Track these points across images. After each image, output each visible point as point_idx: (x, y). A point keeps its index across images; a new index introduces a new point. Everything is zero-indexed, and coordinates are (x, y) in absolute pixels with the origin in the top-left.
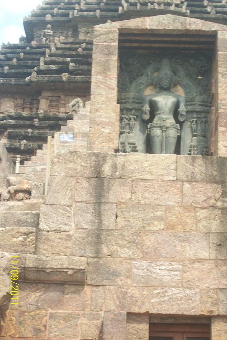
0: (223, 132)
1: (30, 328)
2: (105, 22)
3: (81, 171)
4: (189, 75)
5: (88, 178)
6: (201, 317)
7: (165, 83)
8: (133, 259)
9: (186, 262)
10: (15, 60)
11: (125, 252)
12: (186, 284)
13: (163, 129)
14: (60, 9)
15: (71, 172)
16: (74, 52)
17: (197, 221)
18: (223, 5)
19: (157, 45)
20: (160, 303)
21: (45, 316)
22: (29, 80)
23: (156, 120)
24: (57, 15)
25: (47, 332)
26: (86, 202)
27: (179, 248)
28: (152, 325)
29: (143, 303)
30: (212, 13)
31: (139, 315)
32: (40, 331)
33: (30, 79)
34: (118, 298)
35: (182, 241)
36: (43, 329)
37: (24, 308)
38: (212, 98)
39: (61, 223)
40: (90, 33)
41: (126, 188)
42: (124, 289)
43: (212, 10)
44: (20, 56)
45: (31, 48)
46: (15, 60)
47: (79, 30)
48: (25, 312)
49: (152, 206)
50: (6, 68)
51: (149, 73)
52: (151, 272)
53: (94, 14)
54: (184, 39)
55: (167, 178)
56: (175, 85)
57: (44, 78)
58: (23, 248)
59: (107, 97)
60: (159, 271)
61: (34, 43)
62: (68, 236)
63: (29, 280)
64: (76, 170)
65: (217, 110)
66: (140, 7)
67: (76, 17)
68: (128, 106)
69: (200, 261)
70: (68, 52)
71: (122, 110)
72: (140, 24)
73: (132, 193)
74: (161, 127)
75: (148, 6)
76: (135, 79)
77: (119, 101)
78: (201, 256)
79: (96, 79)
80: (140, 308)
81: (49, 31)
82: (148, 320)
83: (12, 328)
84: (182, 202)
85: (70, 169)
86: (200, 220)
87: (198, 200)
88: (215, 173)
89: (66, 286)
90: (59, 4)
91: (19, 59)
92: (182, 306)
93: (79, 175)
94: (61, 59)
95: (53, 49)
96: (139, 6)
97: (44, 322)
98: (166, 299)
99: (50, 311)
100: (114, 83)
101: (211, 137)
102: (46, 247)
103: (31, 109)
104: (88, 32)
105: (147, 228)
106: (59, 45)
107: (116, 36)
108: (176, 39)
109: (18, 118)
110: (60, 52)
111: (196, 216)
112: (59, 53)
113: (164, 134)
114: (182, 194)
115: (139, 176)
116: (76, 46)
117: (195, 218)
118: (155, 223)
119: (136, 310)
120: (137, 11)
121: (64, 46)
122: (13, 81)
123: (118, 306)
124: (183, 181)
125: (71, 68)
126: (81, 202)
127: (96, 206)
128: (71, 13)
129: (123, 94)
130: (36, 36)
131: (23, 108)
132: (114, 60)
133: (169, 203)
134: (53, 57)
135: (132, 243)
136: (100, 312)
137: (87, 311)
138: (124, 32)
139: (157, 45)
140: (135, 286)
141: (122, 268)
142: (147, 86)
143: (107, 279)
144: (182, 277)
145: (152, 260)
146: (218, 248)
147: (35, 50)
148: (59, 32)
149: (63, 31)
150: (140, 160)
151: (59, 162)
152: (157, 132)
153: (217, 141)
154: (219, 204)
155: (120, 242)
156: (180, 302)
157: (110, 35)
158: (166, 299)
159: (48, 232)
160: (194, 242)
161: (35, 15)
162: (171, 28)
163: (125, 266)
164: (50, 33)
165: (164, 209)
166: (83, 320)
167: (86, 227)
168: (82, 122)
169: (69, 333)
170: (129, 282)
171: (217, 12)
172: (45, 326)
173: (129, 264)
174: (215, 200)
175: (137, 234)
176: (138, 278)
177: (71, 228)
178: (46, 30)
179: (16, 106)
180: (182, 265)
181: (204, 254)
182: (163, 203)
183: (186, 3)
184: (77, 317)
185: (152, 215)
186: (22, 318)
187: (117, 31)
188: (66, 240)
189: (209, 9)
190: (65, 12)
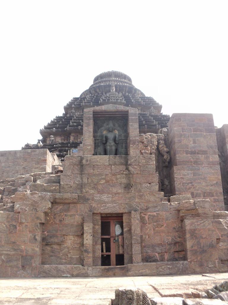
0: (132, 147)
1: (58, 220)
2: (94, 107)
3: (75, 163)
4: (119, 126)
5: (78, 165)
6: (119, 214)
7: (111, 129)
8: (94, 194)
9: (113, 194)
11: (92, 191)
12: (113, 202)
13: (111, 146)
15: (71, 163)
17: (117, 179)
19: (107, 116)
20: (104, 209)
21: (63, 215)
23: (108, 144)
24: (76, 105)
25: (64, 221)
26: (77, 174)
27: (111, 189)
28: (102, 217)
29: (98, 209)
31: (97, 214)
32: (61, 221)
33: (67, 129)
34: (89, 208)
35: (111, 186)
36: (63, 220)
37: (56, 213)
38: (128, 135)
39: (68, 182)
41: (91, 168)
42: (91, 205)
43: (134, 101)
45: (67, 117)
48: (56, 214)
49: (101, 175)
50: (58, 125)
51: (105, 126)
52: (101, 198)
54: (117, 113)
55: (106, 164)
56: (114, 130)
58: (55, 191)
59: (89, 135)
60: (103, 198)
61: (68, 115)
62: (71, 186)
63: (57, 202)
64: (73, 162)
65: (129, 139)
68: (97, 138)
69: (118, 193)
71: (95, 140)
72: (100, 108)
73: (93, 170)
74: (110, 146)
76: (100, 128)
77: (94, 137)
78: (119, 192)
79: (85, 128)
80: (97, 211)
82: (100, 216)
83: (52, 220)
84: (111, 173)
85: (71, 162)
86: (118, 179)
87: (117, 172)
88: (123, 162)
89: (70, 204)
91: (62, 122)
92: (112, 210)
93: (74, 164)
95: (75, 117)
97: (63, 218)
98: (106, 207)
99: (65, 213)
100: (92, 130)
101: (128, 148)
102: (63, 191)
103: (67, 140)
105: (99, 183)
106: (77, 116)
107: (92, 113)
108: (114, 113)
109: (62, 143)
110: (77, 119)
111: (116, 177)
113: (111, 148)
114: (111, 170)
115: (96, 164)
117: (116, 178)
118: (102, 180)
119: (96, 212)
123: (89, 211)
124: (111, 165)
126: (75, 174)
127: (81, 175)
129: (95, 134)
131: (64, 140)
132: (92, 121)
133: (106, 173)
135: (94, 188)
136: (83, 213)
137: (78, 213)
138: (95, 111)
139: (107, 116)
140: (95, 204)
141: (90, 197)
142: (104, 131)
143: (86, 201)
144: (112, 200)
145: (101, 194)
146: (125, 189)
147: (68, 118)
150: (96, 158)
151: (67, 160)
152: (108, 148)
153: (130, 150)
154: (125, 173)
155: (90, 188)
156: (111, 209)
157: (90, 113)
158: (106, 207)
159: (63, 185)
160: (116, 187)
161: (68, 105)
162: (112, 109)
163: (91, 196)
165: (105, 175)
166: (77, 216)
167: (77, 183)
169: (72, 221)
170: (93, 202)
172: (63, 219)
173: (93, 195)
174: (123, 171)
175: (96, 185)
176: (96, 201)
177: (72, 183)
178: (72, 111)
179: (61, 139)
180: (112, 195)
181: (120, 191)
182: (105, 173)
183: (124, 99)
184: (75, 215)
185: (101, 177)
186: (55, 217)
187: (92, 111)
188: (70, 188)
189: (133, 101)
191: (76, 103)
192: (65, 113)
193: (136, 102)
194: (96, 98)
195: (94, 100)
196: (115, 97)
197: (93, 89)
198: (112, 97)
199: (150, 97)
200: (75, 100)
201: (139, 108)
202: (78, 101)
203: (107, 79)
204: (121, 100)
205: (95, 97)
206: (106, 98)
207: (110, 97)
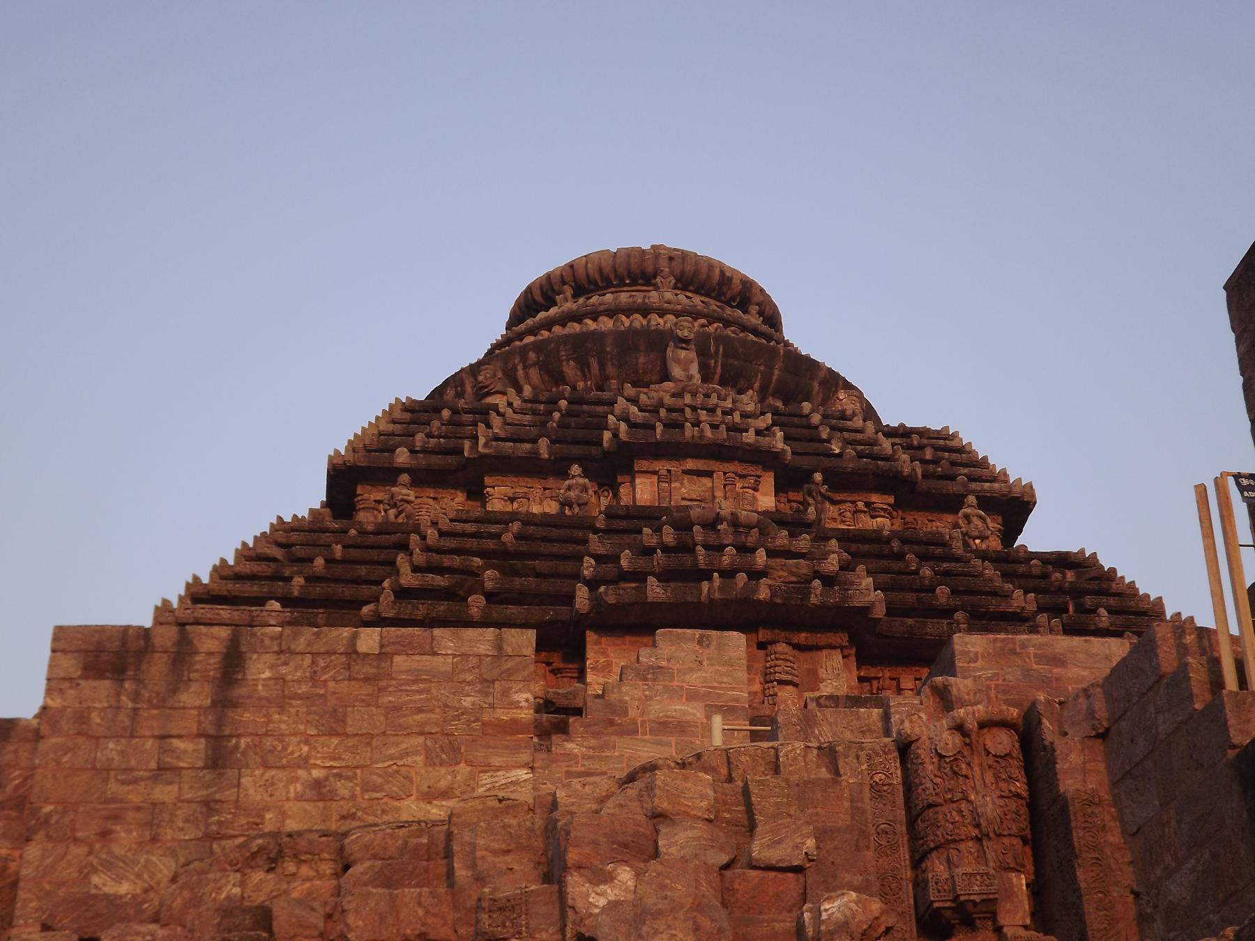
10: (320, 561)
14: (429, 435)
16: (490, 544)
18: (869, 438)
22: (372, 613)
24: (425, 451)
44: (334, 553)
45: (362, 532)
46: (320, 561)
47: (488, 492)
57: (418, 609)
67: (483, 456)
70: (472, 544)
75: (686, 429)
81: (405, 491)
90: (429, 425)
91: (330, 561)
94: (456, 561)
95: (431, 533)
96: (659, 428)
104: (511, 495)
106: (445, 525)
110: (451, 543)
116: (494, 529)
120: (658, 443)
122: (320, 616)
125: (489, 585)
128: (467, 444)
130: (361, 506)
134: (434, 555)
147: (372, 539)
149: (440, 496)
168: (649, 688)
178: (394, 489)
191: (419, 437)
192: (325, 500)
193: (860, 455)
194: (568, 414)
195: (561, 425)
196: (719, 412)
197: (532, 356)
198: (694, 409)
200: (407, 416)
201: (875, 498)
202: (436, 424)
203: (624, 297)
205: (563, 403)
206: (654, 410)
207: (681, 411)
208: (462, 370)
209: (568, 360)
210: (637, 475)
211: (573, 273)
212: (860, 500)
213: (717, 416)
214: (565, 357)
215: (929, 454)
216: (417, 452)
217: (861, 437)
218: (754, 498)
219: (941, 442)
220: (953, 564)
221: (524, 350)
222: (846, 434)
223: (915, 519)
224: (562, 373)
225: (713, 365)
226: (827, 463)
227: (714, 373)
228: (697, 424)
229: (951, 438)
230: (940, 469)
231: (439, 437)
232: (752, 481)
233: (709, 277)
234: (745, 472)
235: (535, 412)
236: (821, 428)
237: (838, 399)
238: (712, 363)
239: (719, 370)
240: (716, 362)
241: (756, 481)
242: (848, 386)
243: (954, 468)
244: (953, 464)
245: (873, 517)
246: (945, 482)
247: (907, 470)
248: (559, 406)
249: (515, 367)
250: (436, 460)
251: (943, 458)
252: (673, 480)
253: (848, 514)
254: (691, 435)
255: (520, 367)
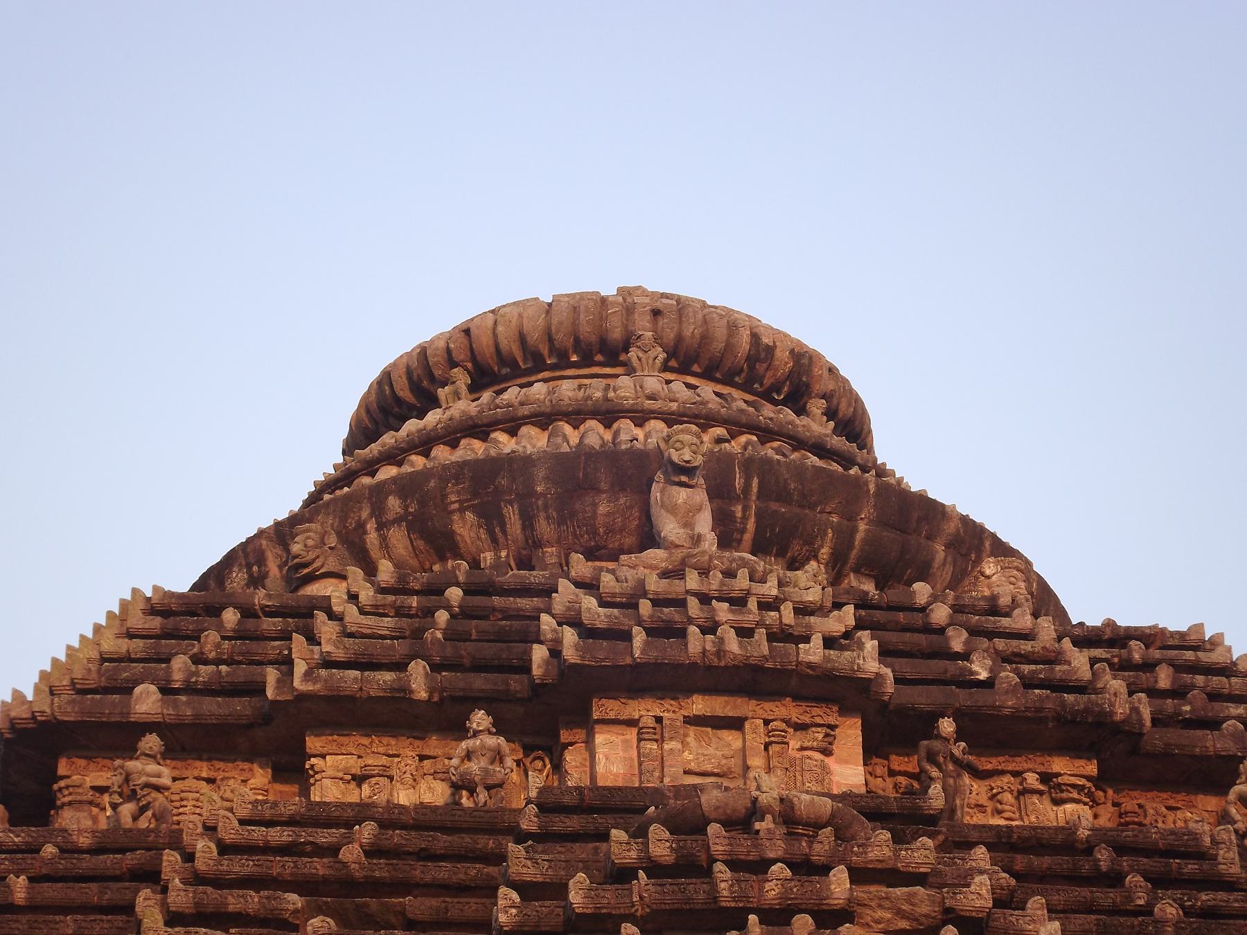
14: (199, 660)
16: (319, 867)
18: (1044, 648)
24: (190, 689)
30: (1001, 686)
40: (374, 780)
44: (12, 893)
45: (69, 850)
47: (312, 766)
53: (399, 679)
66: (646, 643)
67: (302, 697)
70: (282, 866)
75: (691, 638)
81: (152, 767)
90: (198, 639)
94: (252, 901)
95: (204, 849)
96: (639, 638)
106: (230, 831)
110: (242, 866)
112: (237, 869)
116: (325, 837)
120: (636, 667)
121: (258, 834)
130: (66, 799)
134: (209, 889)
147: (88, 863)
148: (198, 778)
149: (220, 776)
164: (159, 776)
171: (1029, 683)
178: (132, 765)
190: (228, 674)
191: (180, 666)
194: (465, 613)
195: (452, 635)
196: (752, 604)
197: (394, 504)
198: (705, 599)
199: (1199, 628)
200: (156, 623)
201: (1059, 765)
202: (211, 637)
203: (567, 389)
204: (829, 642)
206: (630, 604)
207: (680, 603)
208: (261, 533)
209: (462, 510)
210: (597, 728)
211: (471, 345)
212: (1029, 770)
213: (750, 612)
214: (456, 506)
215: (1164, 678)
216: (176, 692)
217: (1029, 648)
218: (825, 770)
219: (1189, 655)
220: (1222, 895)
221: (379, 492)
222: (1000, 644)
223: (1140, 806)
224: (451, 535)
225: (739, 515)
226: (963, 697)
227: (743, 531)
228: (710, 628)
229: (1208, 646)
230: (1188, 708)
231: (218, 662)
232: (820, 736)
233: (729, 347)
234: (806, 719)
235: (400, 612)
236: (950, 632)
237: (982, 574)
238: (738, 510)
239: (751, 525)
240: (745, 509)
241: (827, 735)
242: (1002, 550)
243: (1217, 705)
244: (1214, 696)
245: (1057, 802)
246: (1199, 733)
247: (1121, 711)
248: (448, 600)
249: (361, 526)
250: (213, 707)
251: (1193, 686)
252: (666, 735)
253: (1008, 797)
254: (699, 649)
255: (371, 526)
